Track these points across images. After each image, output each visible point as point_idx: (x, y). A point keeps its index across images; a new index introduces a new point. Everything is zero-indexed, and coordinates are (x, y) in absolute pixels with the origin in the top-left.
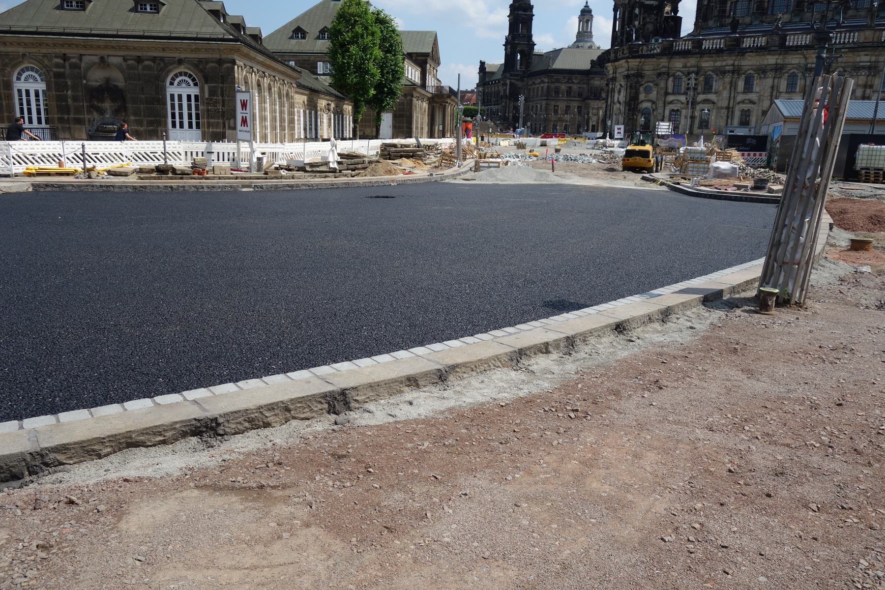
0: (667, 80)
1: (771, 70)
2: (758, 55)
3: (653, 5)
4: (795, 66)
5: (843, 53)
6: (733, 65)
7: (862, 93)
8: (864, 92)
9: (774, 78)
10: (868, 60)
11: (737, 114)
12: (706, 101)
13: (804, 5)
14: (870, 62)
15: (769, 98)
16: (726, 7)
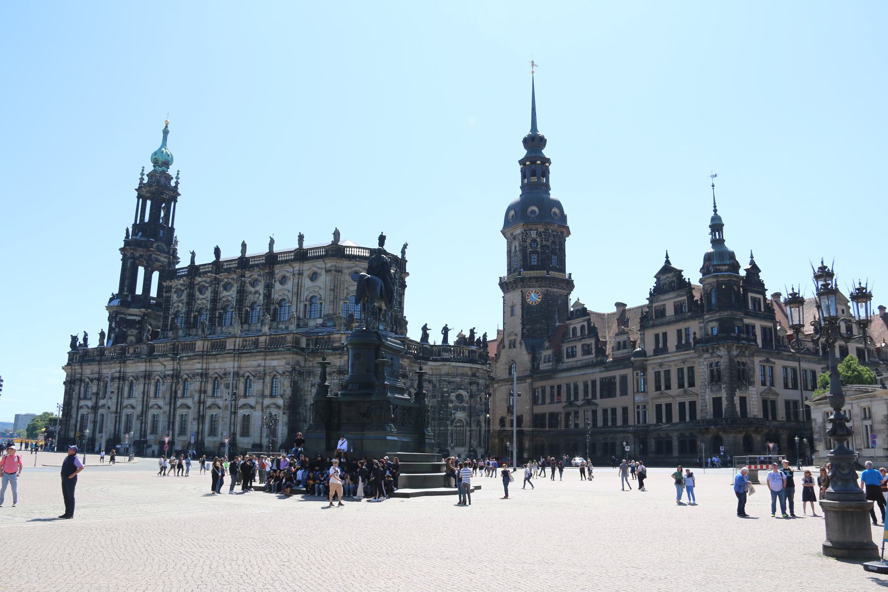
0: (80, 386)
1: (141, 377)
2: (134, 363)
3: (134, 320)
4: (159, 373)
5: (186, 360)
6: (120, 372)
7: (198, 398)
8: (200, 397)
9: (145, 384)
10: (200, 368)
11: (124, 418)
12: (103, 406)
13: (215, 320)
14: (202, 369)
15: (141, 403)
16: (168, 322)
